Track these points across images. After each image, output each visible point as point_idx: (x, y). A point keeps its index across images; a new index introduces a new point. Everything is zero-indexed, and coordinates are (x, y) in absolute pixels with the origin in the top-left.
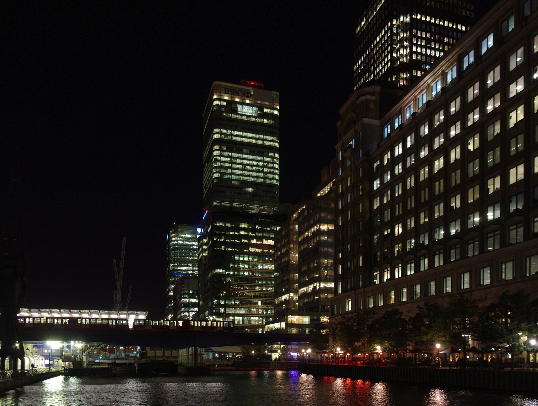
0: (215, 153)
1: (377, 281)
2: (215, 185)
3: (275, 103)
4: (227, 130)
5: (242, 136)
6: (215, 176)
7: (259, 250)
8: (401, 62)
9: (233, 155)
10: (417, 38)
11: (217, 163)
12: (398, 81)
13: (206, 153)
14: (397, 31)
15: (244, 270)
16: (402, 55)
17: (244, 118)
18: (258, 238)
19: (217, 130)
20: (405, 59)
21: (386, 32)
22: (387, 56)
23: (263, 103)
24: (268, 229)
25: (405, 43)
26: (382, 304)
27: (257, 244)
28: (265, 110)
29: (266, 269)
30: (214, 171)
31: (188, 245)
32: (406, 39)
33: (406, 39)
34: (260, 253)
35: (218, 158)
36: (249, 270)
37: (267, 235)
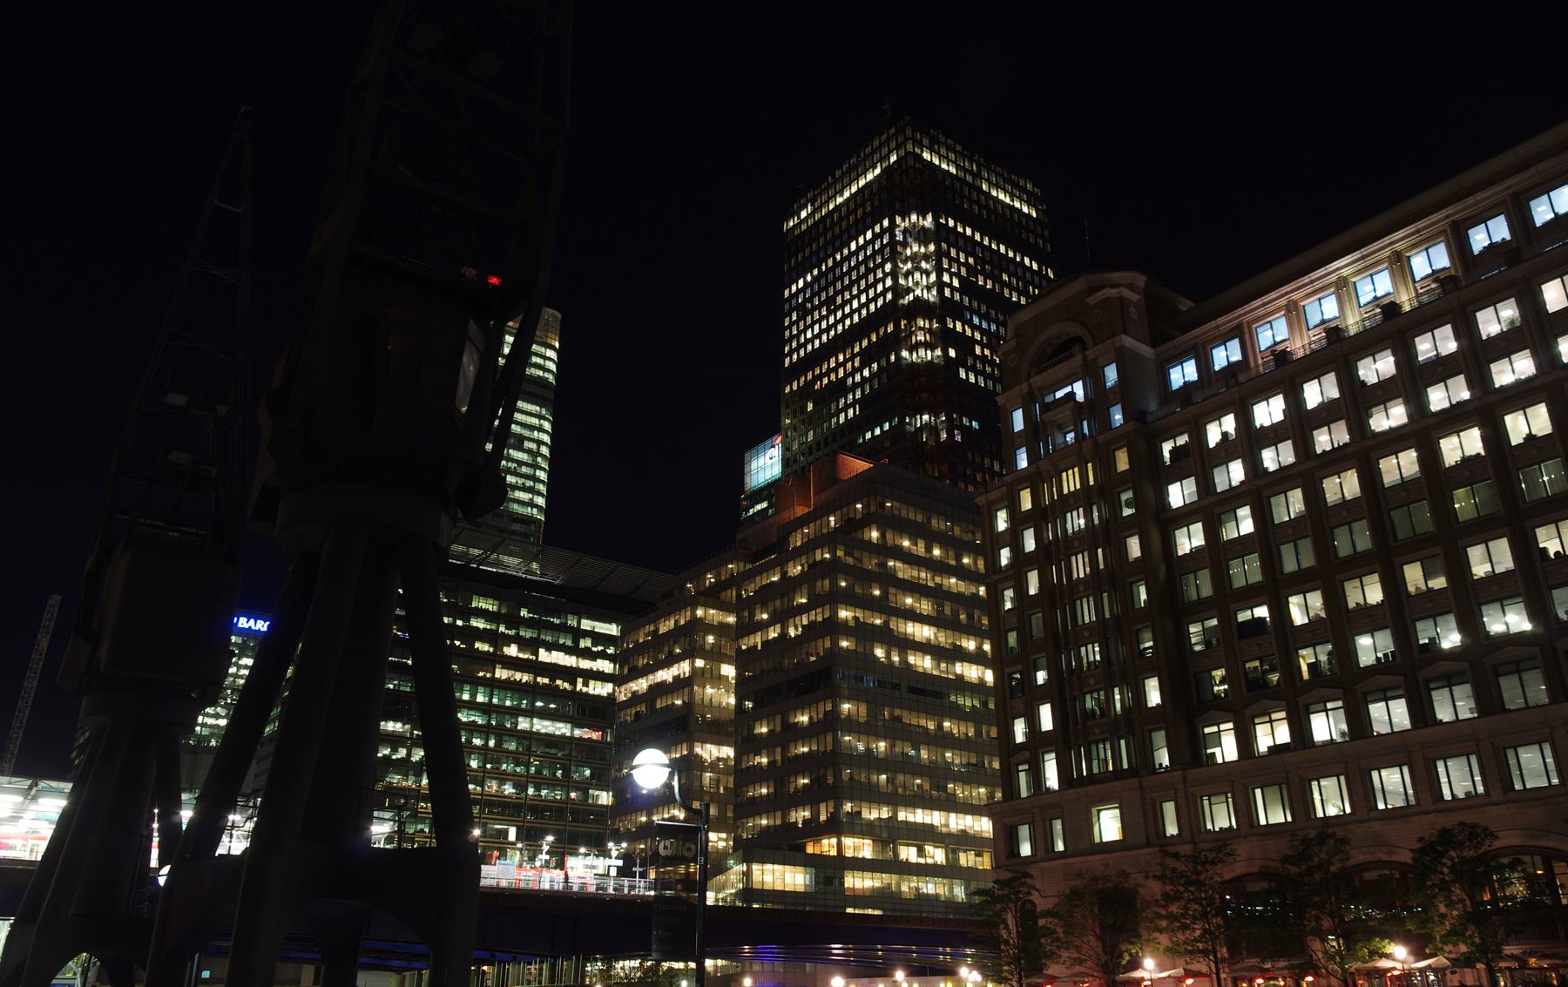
7: (526, 678)
8: (917, 298)
10: (951, 260)
16: (917, 284)
18: (523, 644)
21: (875, 236)
24: (557, 621)
27: (517, 658)
29: (538, 733)
32: (926, 257)
33: (926, 257)
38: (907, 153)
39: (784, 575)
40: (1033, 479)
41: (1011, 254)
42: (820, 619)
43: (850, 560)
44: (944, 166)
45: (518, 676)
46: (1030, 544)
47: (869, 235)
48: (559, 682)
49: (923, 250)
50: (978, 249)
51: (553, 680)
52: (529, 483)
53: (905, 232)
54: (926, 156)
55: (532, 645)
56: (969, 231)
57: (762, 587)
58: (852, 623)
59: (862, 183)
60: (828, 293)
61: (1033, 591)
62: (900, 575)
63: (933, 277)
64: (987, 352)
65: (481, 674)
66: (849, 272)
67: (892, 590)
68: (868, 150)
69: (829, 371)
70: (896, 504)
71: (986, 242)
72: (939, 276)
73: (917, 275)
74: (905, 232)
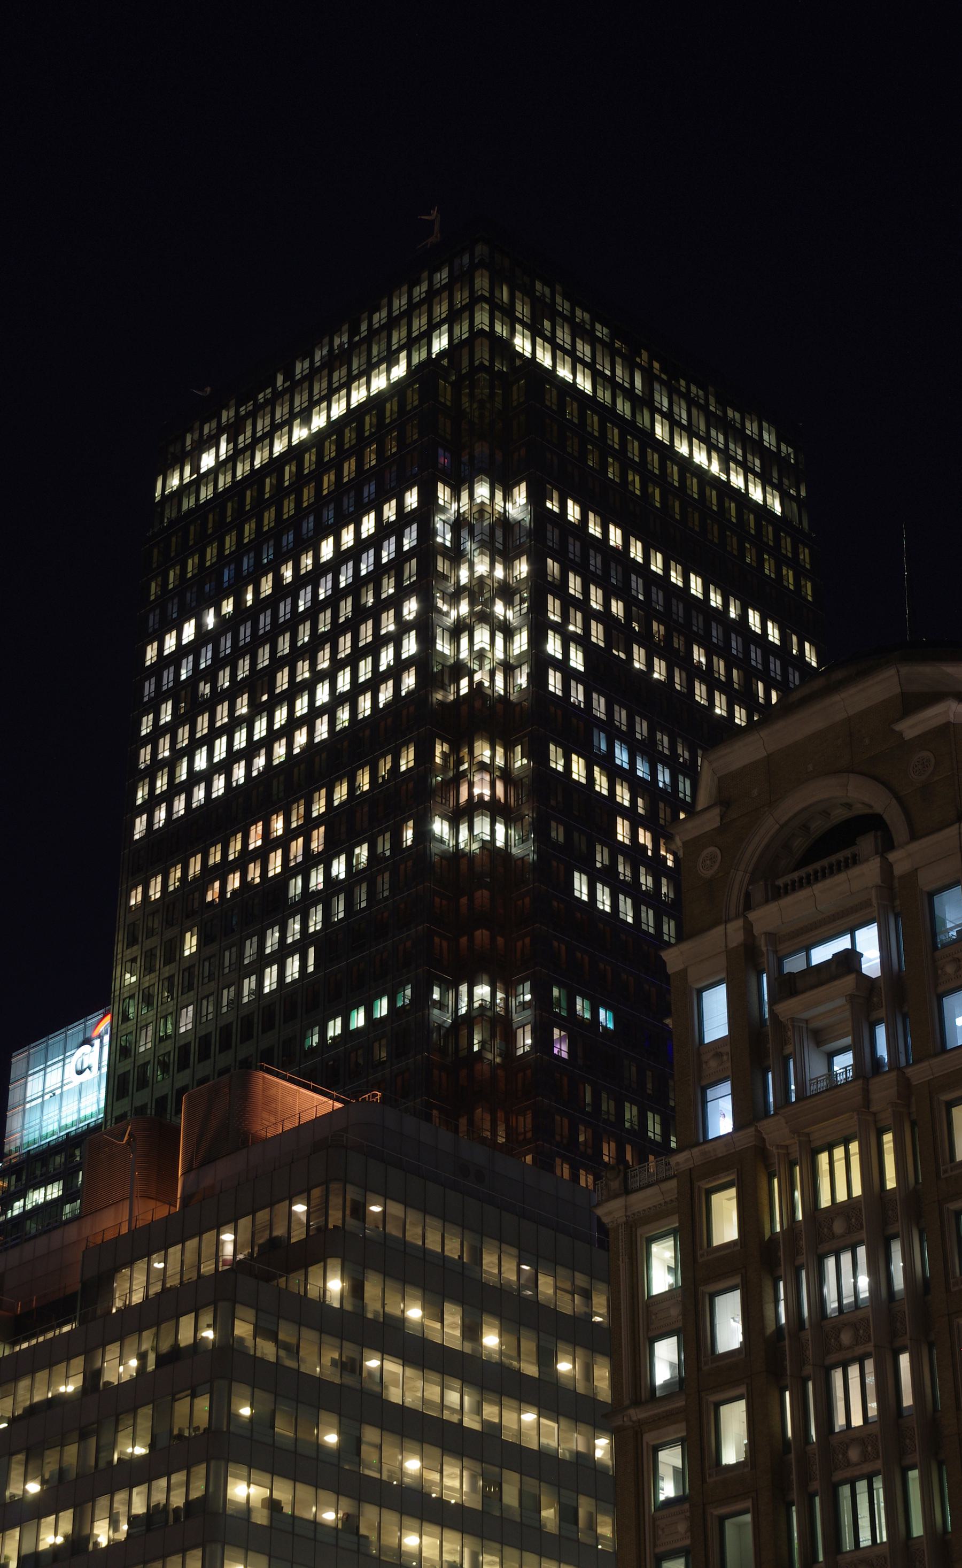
8: (477, 689)
10: (568, 603)
21: (384, 531)
32: (506, 592)
33: (506, 592)
38: (475, 334)
39: (92, 1377)
40: (747, 1165)
41: (716, 600)
42: (178, 1501)
43: (267, 1350)
44: (564, 372)
46: (730, 1333)
47: (368, 525)
49: (499, 573)
50: (637, 584)
54: (522, 344)
56: (615, 537)
57: (33, 1410)
58: (261, 1518)
59: (359, 395)
61: (731, 1454)
62: (394, 1395)
63: (521, 642)
64: (644, 837)
66: (313, 613)
67: (370, 1434)
68: (379, 318)
69: (246, 857)
70: (396, 1209)
71: (657, 566)
72: (537, 641)
73: (482, 636)
74: (458, 525)
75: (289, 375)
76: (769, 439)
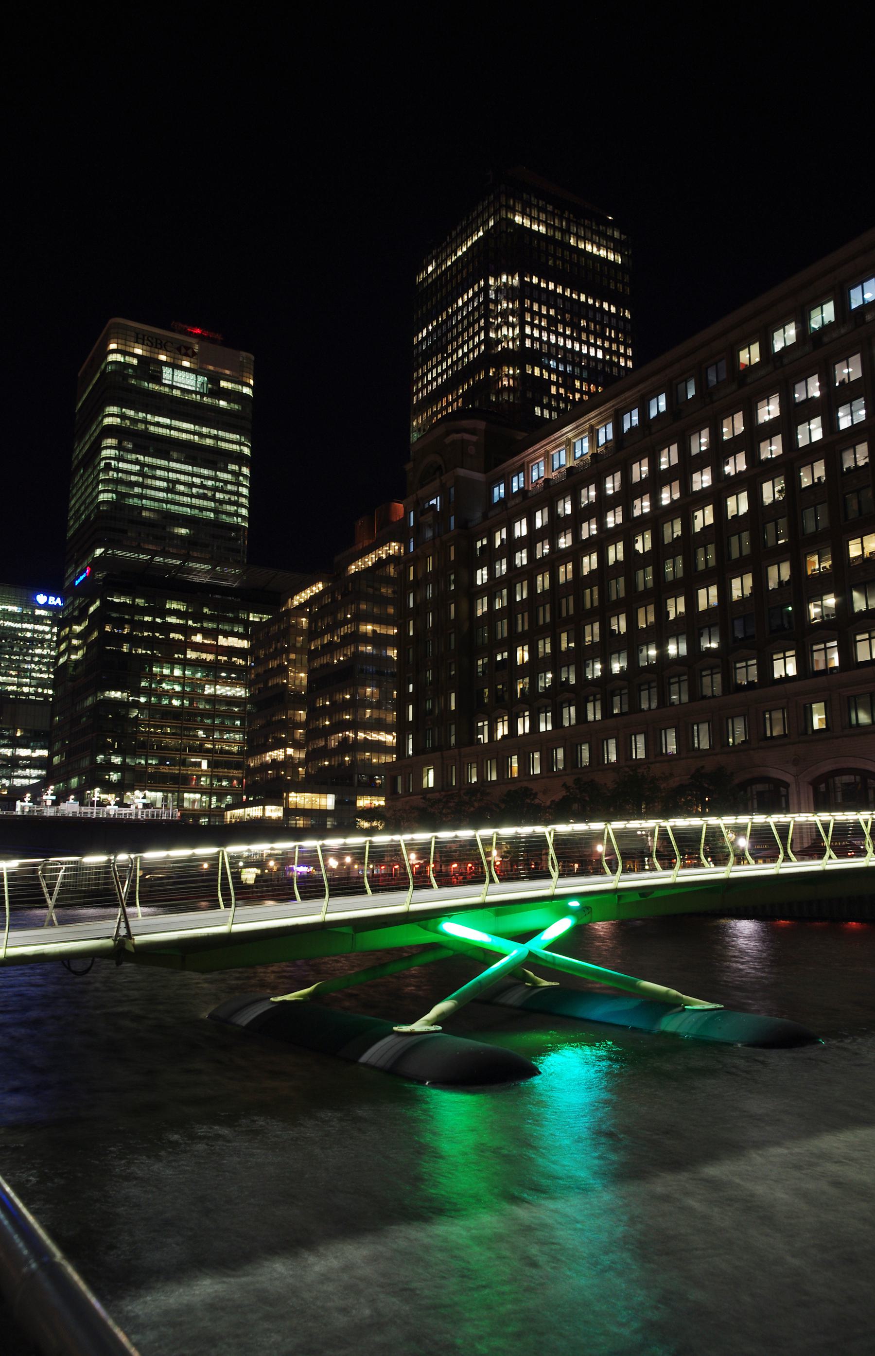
0: (105, 453)
1: (484, 738)
2: (100, 515)
3: (245, 374)
4: (137, 411)
5: (170, 427)
6: (103, 497)
7: (210, 657)
8: (503, 348)
9: (148, 460)
10: (534, 314)
11: (111, 473)
12: (498, 377)
13: (81, 450)
14: (496, 296)
15: (172, 695)
16: (506, 337)
17: (176, 393)
18: (206, 633)
19: (114, 410)
20: (511, 344)
22: (478, 333)
23: (220, 370)
25: (511, 319)
26: (494, 778)
27: (203, 644)
28: (223, 384)
30: (101, 487)
31: (10, 628)
34: (211, 662)
35: (113, 463)
36: (181, 696)
37: (227, 628)
41: (590, 301)
45: (204, 656)
47: (471, 293)
48: (234, 659)
49: (511, 306)
50: (559, 301)
51: (230, 658)
52: (234, 498)
53: (498, 290)
55: (212, 634)
56: (551, 286)
59: (475, 238)
60: (439, 346)
63: (517, 331)
65: (176, 656)
66: (456, 325)
69: (443, 408)
71: (568, 293)
72: (522, 330)
75: (451, 237)
76: (616, 235)
